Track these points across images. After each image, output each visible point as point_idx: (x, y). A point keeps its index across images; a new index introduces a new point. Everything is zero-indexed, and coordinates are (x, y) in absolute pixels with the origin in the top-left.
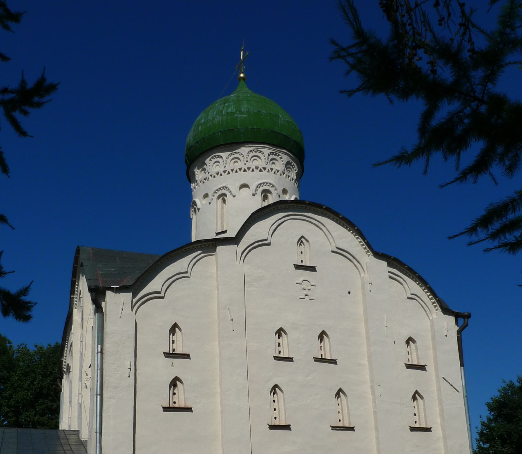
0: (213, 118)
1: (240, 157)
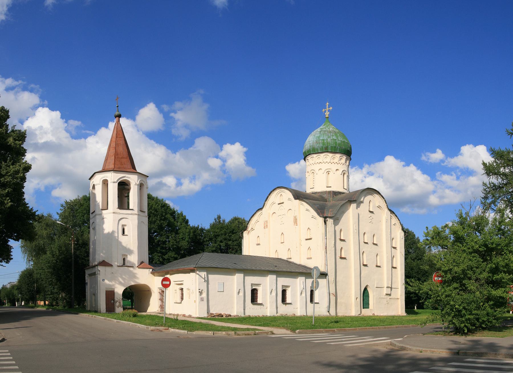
0: (327, 139)
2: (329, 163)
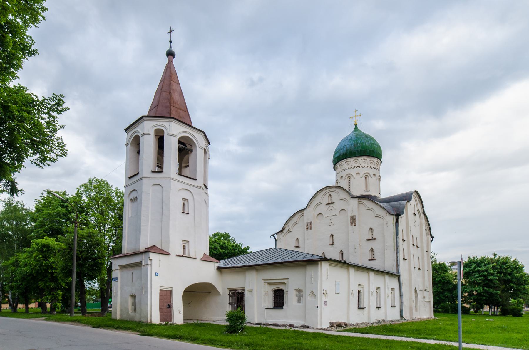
1: (373, 162)
2: (367, 167)
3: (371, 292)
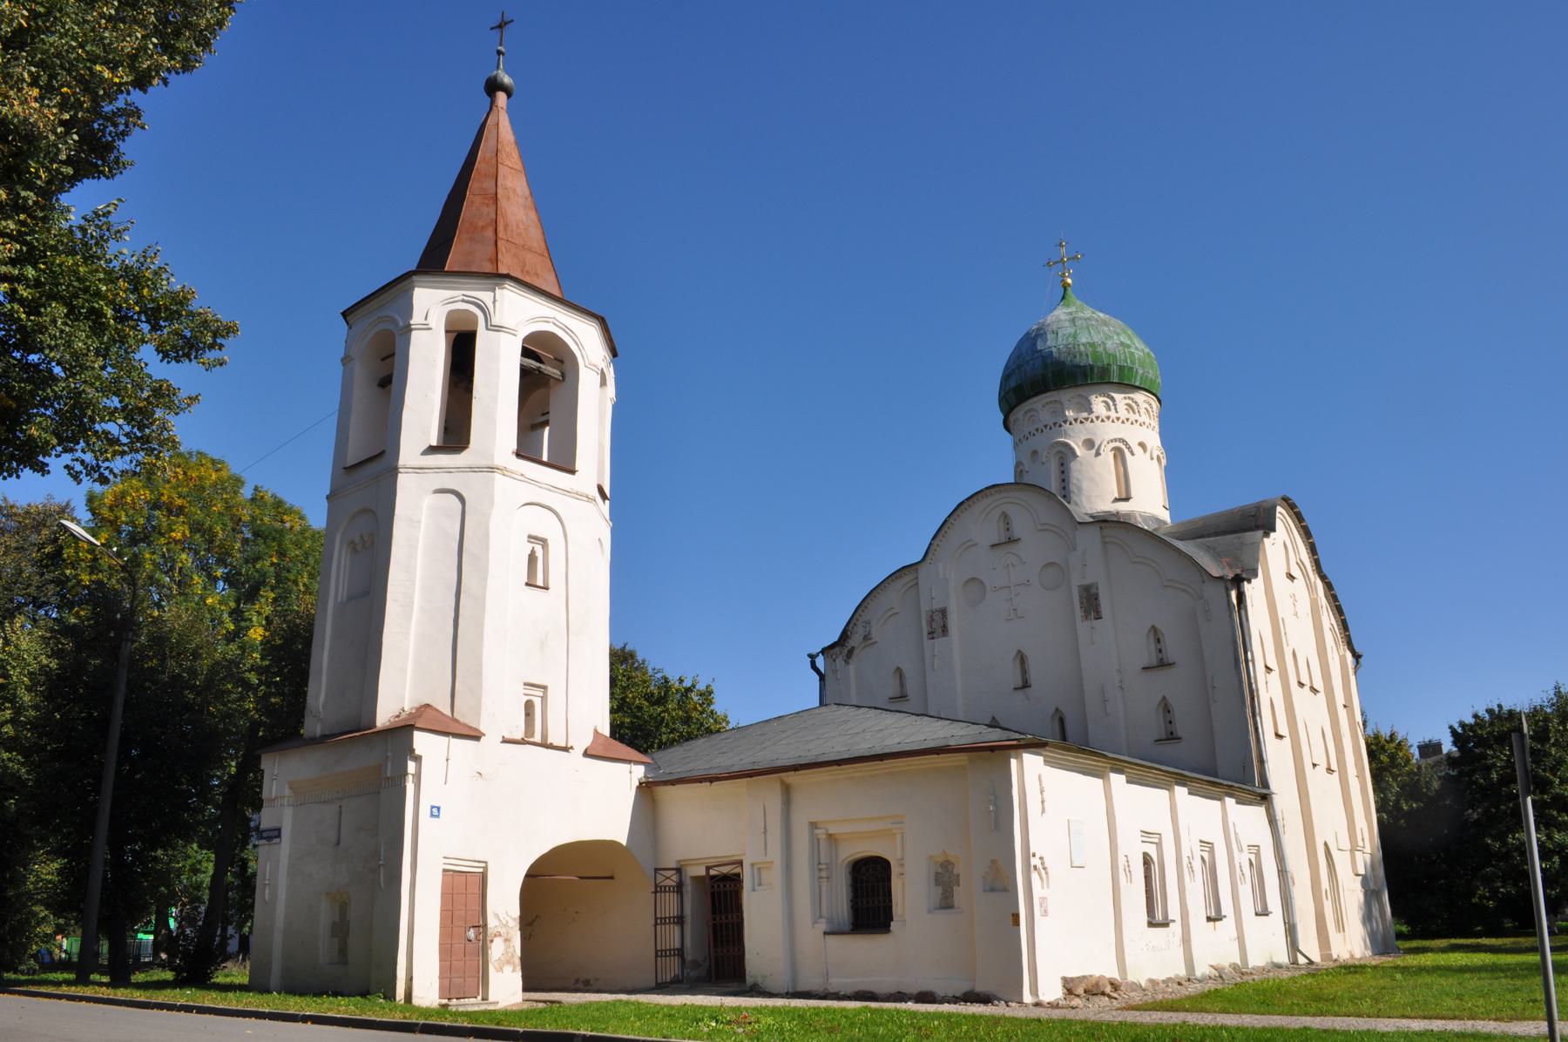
2: (1115, 420)
3: (1185, 861)
